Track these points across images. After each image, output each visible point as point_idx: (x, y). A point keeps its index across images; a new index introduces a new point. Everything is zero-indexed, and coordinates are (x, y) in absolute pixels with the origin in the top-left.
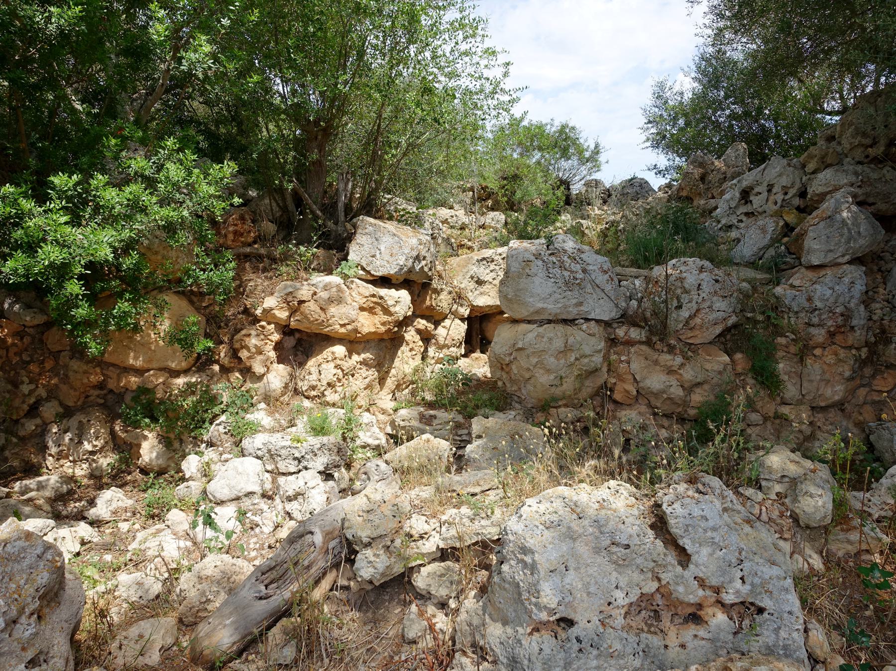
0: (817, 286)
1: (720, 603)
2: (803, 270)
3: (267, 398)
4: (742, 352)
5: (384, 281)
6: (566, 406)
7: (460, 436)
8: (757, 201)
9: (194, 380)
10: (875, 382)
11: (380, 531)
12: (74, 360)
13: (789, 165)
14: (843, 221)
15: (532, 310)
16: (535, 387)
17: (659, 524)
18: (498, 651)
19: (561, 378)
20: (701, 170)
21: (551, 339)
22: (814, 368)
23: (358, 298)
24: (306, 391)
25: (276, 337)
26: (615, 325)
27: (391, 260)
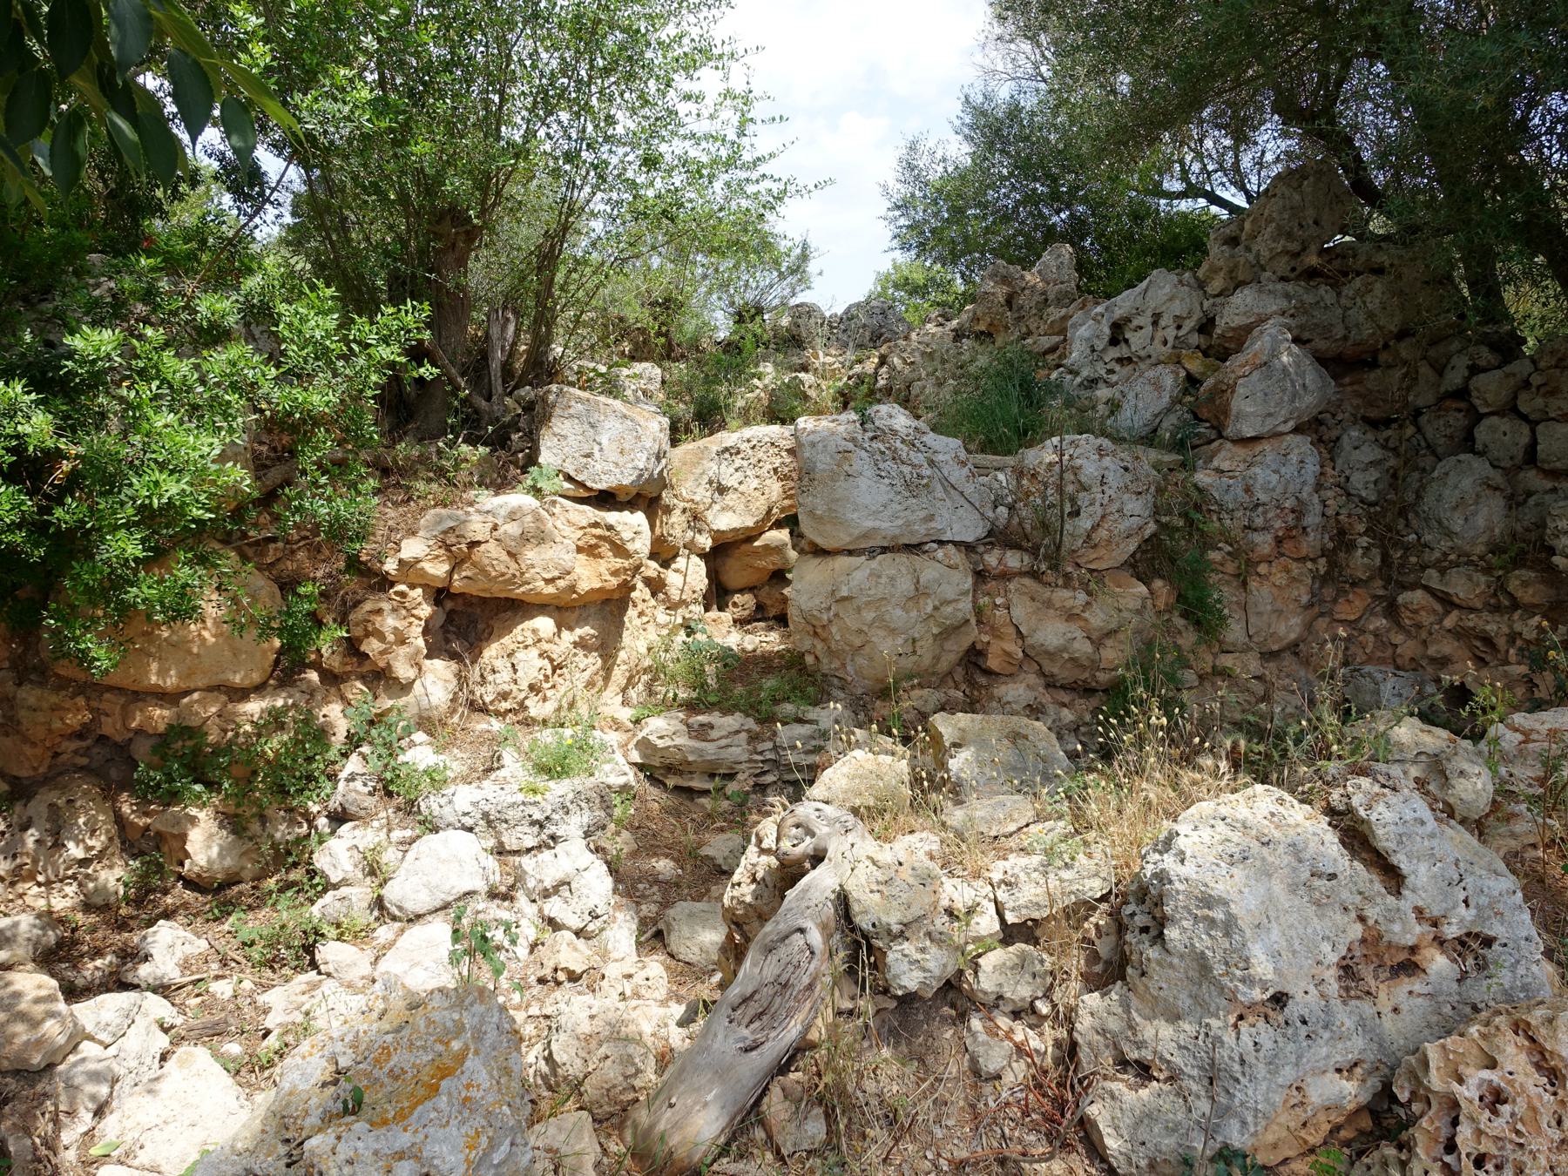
0: (1257, 470)
1: (1440, 942)
2: (1229, 445)
3: (426, 723)
4: (1162, 577)
5: (605, 499)
6: (921, 686)
7: (761, 753)
8: (1137, 340)
9: (280, 703)
10: (1338, 608)
11: (916, 911)
12: (27, 687)
13: (1180, 282)
14: (1285, 369)
15: (857, 532)
16: (871, 659)
17: (1355, 835)
18: (1177, 1060)
19: (914, 641)
20: (1005, 289)
21: (892, 579)
22: (1261, 593)
23: (568, 531)
24: (492, 702)
26: (981, 549)
27: (621, 461)
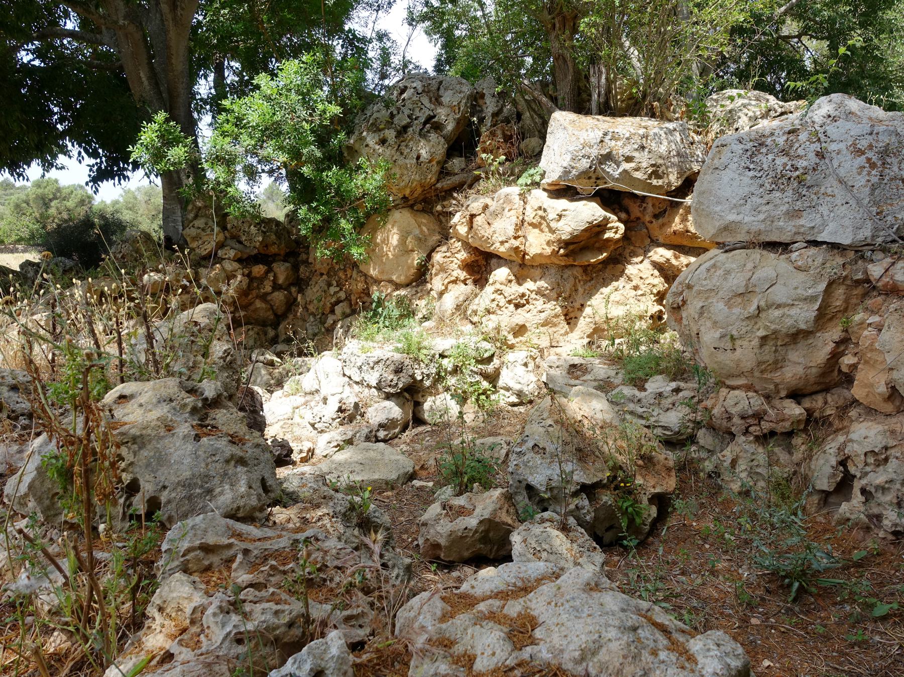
6: (749, 388)
19: (733, 338)
21: (728, 272)
25: (463, 255)
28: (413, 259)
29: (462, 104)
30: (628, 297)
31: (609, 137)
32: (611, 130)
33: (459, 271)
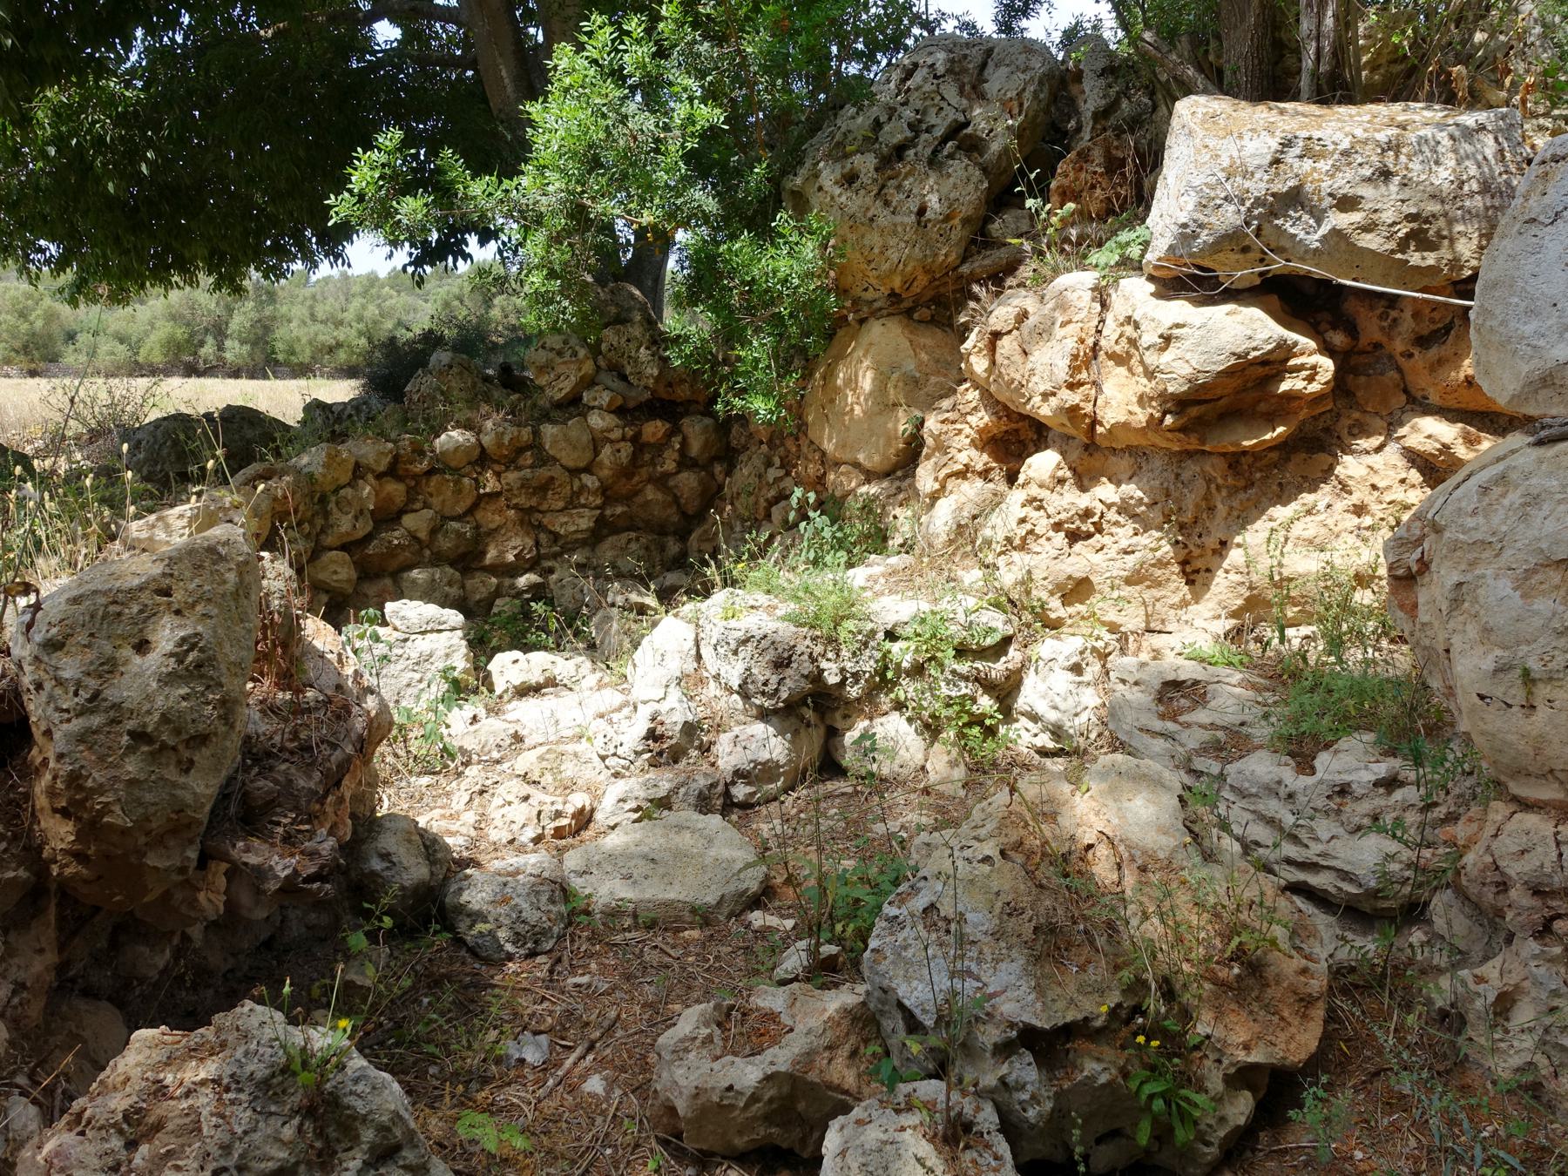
19: (1528, 678)
25: (981, 419)
28: (897, 421)
29: (1027, 95)
30: (1326, 535)
31: (1297, 151)
32: (1305, 134)
33: (974, 453)
